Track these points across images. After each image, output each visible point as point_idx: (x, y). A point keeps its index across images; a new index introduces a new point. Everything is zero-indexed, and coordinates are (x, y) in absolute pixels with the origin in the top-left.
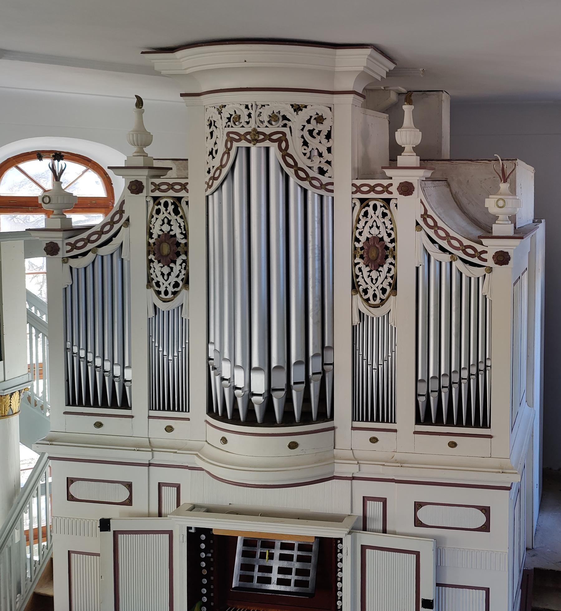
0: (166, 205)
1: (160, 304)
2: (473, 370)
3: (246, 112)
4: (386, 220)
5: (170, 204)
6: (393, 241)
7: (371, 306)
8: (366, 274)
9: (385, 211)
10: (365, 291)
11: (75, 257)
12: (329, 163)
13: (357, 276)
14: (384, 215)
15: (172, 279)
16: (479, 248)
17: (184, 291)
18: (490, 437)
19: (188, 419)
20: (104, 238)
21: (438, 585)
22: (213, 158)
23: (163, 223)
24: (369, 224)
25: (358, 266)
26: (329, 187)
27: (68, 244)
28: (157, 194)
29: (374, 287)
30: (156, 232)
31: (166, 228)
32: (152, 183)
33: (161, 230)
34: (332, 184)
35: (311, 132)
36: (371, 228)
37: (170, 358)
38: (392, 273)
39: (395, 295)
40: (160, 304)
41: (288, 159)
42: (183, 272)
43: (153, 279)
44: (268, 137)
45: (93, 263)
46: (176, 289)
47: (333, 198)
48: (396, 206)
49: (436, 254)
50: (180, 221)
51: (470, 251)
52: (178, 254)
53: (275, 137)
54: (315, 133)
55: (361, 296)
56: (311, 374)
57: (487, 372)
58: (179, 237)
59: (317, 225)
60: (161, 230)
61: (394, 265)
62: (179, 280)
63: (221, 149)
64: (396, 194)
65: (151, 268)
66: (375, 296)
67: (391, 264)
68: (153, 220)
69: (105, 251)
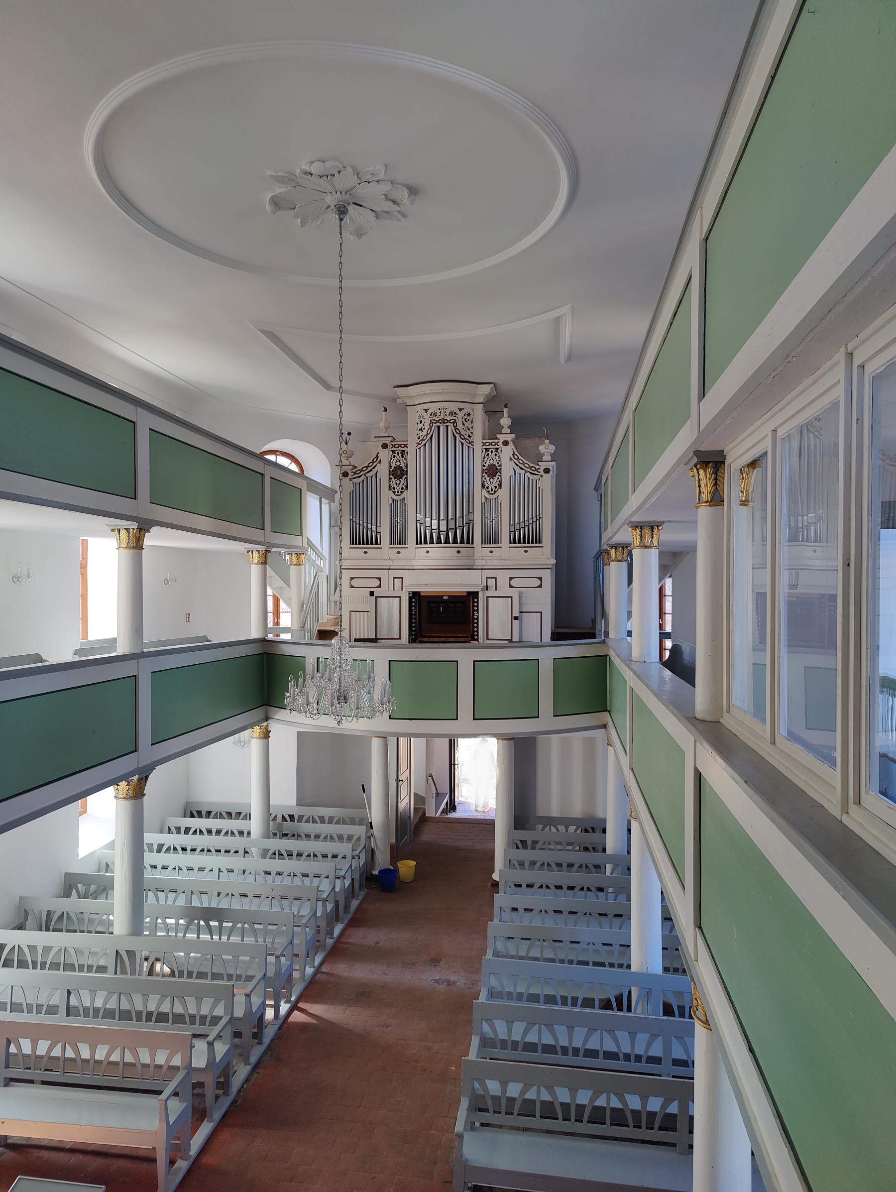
0: (398, 453)
1: (395, 498)
2: (535, 520)
3: (439, 411)
4: (497, 457)
6: (500, 466)
7: (490, 494)
8: (488, 480)
10: (488, 488)
11: (355, 478)
12: (472, 433)
13: (484, 482)
14: (496, 455)
15: (401, 486)
16: (537, 467)
17: (406, 491)
18: (542, 547)
20: (369, 469)
21: (520, 612)
22: (422, 431)
23: (397, 461)
24: (489, 459)
26: (472, 443)
27: (352, 472)
28: (394, 449)
29: (492, 486)
30: (393, 465)
31: (398, 463)
32: (392, 444)
33: (396, 464)
34: (473, 442)
35: (465, 419)
36: (490, 460)
37: (399, 521)
38: (499, 479)
40: (395, 498)
42: (405, 483)
43: (391, 487)
44: (449, 421)
45: (363, 481)
47: (473, 448)
48: (501, 451)
49: (518, 470)
50: (404, 460)
51: (533, 469)
52: (403, 475)
53: (451, 421)
54: (467, 420)
56: (464, 523)
57: (541, 520)
58: (404, 467)
59: (467, 462)
60: (396, 464)
61: (500, 476)
63: (427, 427)
66: (492, 490)
67: (499, 475)
68: (392, 460)
69: (368, 475)
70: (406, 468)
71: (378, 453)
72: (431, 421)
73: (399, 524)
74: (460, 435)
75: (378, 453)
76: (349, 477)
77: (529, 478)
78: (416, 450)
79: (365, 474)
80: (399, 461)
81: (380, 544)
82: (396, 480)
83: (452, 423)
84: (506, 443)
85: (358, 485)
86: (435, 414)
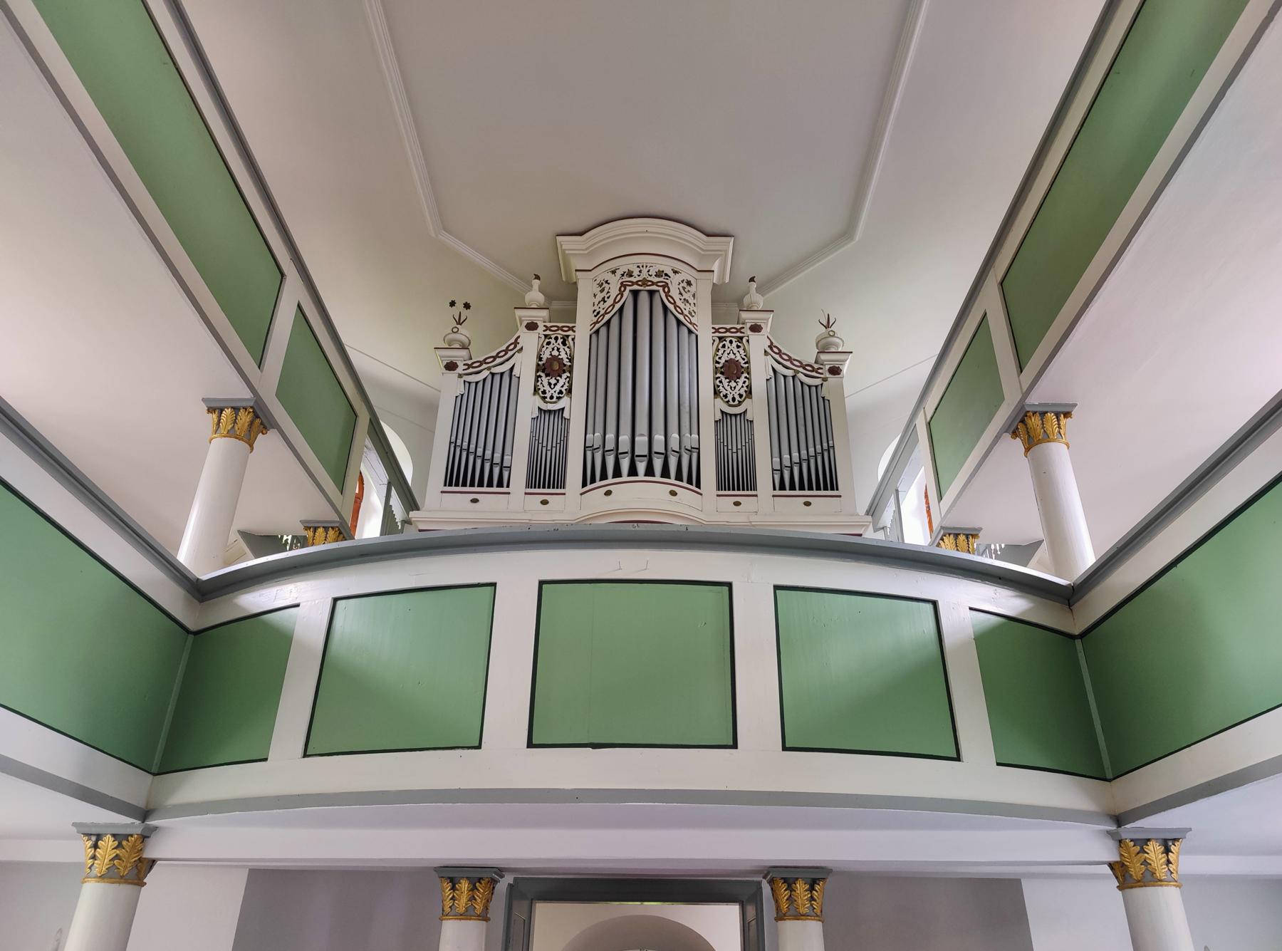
0: (556, 339)
4: (741, 350)
5: (559, 338)
6: (745, 363)
7: (730, 406)
9: (739, 344)
10: (726, 396)
11: (470, 374)
13: (719, 386)
14: (738, 347)
15: (558, 388)
16: (816, 366)
18: (840, 496)
19: (564, 494)
25: (718, 380)
27: (464, 365)
28: (548, 332)
30: (546, 356)
33: (551, 355)
39: (751, 398)
41: (669, 298)
42: (567, 384)
44: (653, 284)
46: (560, 395)
48: (748, 341)
50: (567, 350)
52: (564, 372)
55: (722, 399)
61: (748, 379)
62: (563, 389)
64: (749, 332)
65: (538, 381)
66: (734, 399)
67: (746, 377)
68: (544, 349)
70: (570, 361)
71: (519, 337)
72: (622, 283)
73: (549, 453)
74: (676, 307)
75: (519, 337)
76: (460, 370)
77: (802, 383)
78: (591, 336)
79: (489, 368)
80: (558, 349)
81: (508, 486)
82: (548, 378)
83: (661, 286)
84: (756, 328)
85: (473, 386)
86: (630, 274)
